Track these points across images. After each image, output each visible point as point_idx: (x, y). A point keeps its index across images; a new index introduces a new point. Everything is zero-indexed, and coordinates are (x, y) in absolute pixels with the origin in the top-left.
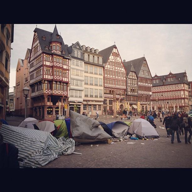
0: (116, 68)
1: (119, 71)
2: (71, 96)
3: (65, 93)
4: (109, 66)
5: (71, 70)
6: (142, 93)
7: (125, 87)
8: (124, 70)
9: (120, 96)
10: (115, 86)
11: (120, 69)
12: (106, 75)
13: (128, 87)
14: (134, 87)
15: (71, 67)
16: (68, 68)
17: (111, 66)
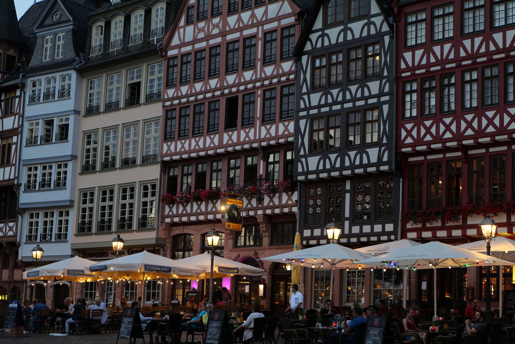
0: (232, 20)
1: (246, 33)
2: (30, 239)
3: (11, 229)
4: (189, 33)
5: (26, 126)
6: (438, 138)
7: (291, 127)
8: (287, 8)
9: (260, 200)
10: (221, 139)
11: (259, 12)
12: (171, 92)
13: (302, 123)
14: (355, 110)
15: (26, 115)
16: (16, 126)
17: (201, 25)
